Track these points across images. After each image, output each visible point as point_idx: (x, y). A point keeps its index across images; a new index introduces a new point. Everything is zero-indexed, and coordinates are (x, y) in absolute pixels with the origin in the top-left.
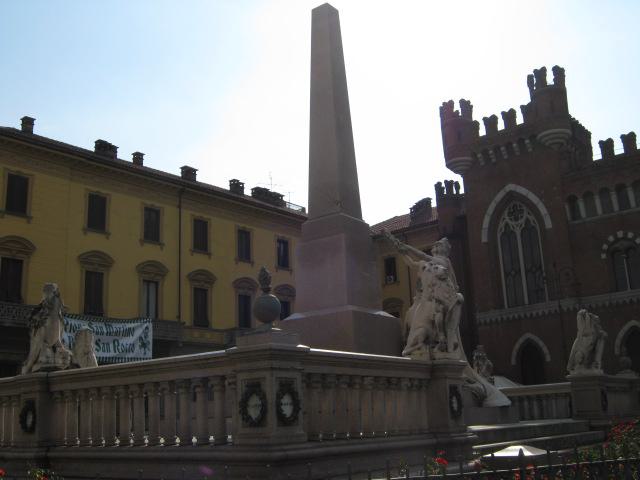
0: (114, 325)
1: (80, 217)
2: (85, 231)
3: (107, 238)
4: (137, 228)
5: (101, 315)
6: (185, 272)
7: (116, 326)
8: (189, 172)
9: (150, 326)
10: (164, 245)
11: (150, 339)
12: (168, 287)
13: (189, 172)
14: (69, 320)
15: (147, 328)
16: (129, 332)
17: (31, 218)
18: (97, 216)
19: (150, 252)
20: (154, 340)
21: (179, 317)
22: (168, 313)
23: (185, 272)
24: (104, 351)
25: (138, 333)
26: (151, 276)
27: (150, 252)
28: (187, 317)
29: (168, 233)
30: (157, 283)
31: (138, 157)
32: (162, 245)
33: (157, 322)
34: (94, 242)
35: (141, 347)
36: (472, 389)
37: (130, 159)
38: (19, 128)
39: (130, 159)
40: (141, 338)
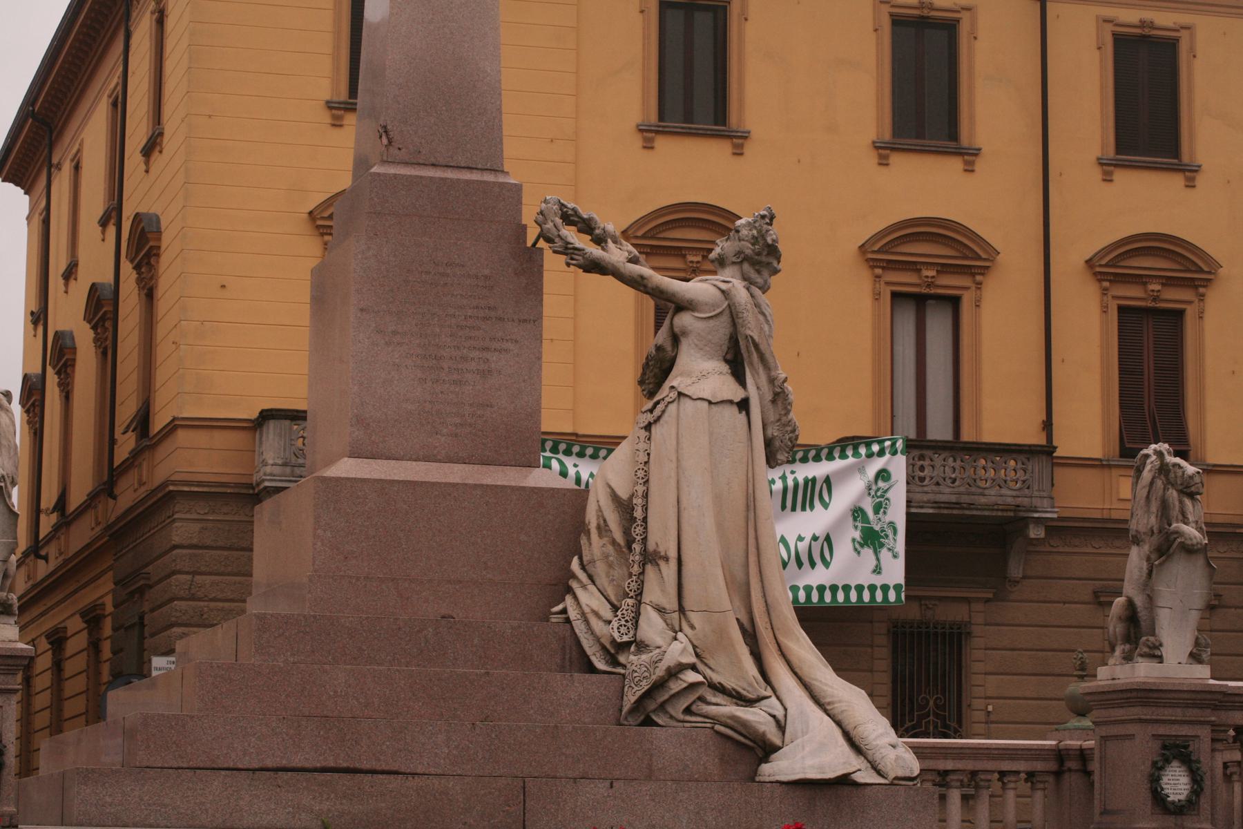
1: (630, 91)
2: (648, 134)
3: (738, 152)
4: (860, 91)
6: (1072, 255)
9: (898, 466)
11: (897, 514)
12: (1001, 316)
14: (569, 462)
15: (883, 474)
16: (807, 495)
19: (924, 188)
20: (911, 518)
21: (1048, 425)
22: (1003, 416)
23: (1072, 255)
25: (848, 494)
26: (926, 276)
27: (924, 188)
28: (1086, 426)
29: (993, 101)
30: (954, 302)
33: (918, 447)
34: (690, 171)
35: (859, 546)
36: (715, 719)
40: (857, 513)
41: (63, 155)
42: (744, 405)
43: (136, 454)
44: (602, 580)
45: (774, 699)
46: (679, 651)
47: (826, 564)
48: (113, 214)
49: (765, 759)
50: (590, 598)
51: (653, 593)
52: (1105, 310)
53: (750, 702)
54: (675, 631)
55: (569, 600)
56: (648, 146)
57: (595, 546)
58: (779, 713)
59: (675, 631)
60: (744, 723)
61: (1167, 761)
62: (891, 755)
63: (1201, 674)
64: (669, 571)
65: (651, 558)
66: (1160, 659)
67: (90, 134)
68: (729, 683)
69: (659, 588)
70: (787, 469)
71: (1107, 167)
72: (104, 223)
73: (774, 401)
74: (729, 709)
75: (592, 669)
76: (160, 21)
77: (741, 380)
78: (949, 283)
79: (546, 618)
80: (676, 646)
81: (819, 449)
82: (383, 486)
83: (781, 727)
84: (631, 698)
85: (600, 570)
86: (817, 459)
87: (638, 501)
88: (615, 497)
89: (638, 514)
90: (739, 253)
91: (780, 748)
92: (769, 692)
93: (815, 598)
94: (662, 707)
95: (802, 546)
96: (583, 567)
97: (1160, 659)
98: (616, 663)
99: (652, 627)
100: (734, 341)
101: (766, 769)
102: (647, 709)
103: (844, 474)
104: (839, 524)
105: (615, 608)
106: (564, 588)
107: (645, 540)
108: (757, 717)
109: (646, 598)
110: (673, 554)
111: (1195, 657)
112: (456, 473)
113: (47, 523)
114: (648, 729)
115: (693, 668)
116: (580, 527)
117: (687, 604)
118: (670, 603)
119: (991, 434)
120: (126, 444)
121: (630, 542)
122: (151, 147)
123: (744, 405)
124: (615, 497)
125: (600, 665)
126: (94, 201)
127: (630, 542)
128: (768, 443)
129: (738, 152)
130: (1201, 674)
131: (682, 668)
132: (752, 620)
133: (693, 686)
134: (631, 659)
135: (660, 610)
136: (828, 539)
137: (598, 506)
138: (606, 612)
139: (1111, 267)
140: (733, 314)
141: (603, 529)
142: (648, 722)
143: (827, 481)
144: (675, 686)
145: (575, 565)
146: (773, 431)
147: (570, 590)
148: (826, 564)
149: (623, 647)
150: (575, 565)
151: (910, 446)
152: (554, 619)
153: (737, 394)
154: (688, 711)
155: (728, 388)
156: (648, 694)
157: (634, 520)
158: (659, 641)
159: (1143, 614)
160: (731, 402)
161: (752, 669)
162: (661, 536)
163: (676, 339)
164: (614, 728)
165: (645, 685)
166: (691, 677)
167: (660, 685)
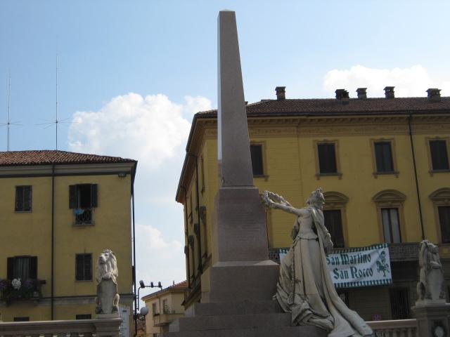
0: (349, 254)
1: (312, 165)
3: (340, 179)
4: (369, 162)
5: (343, 246)
6: (425, 195)
7: (351, 255)
8: (434, 93)
9: (387, 250)
10: (398, 173)
11: (388, 261)
12: (409, 211)
13: (434, 93)
15: (383, 253)
16: (365, 259)
17: (268, 176)
18: (328, 161)
19: (387, 182)
20: (391, 263)
23: (425, 195)
24: (342, 278)
25: (375, 257)
26: (389, 204)
27: (387, 182)
29: (401, 159)
30: (397, 209)
31: (389, 91)
32: (397, 174)
33: (391, 247)
34: (329, 184)
35: (379, 270)
36: (316, 323)
37: (383, 95)
38: (275, 98)
39: (383, 95)
41: (188, 195)
42: (317, 240)
43: (205, 262)
44: (285, 288)
45: (331, 317)
46: (305, 305)
47: (371, 275)
48: (197, 208)
49: (330, 333)
50: (281, 293)
51: (297, 291)
52: (434, 208)
53: (325, 318)
54: (304, 300)
55: (277, 294)
56: (318, 179)
57: (282, 280)
58: (332, 320)
59: (304, 300)
60: (323, 323)
61: (436, 327)
62: (364, 329)
63: (444, 302)
64: (301, 284)
65: (296, 281)
66: (431, 299)
67: (193, 189)
68: (319, 313)
69: (299, 289)
70: (359, 252)
71: (431, 173)
72: (196, 209)
73: (325, 238)
74: (318, 320)
75: (284, 312)
76: (203, 162)
77: (316, 234)
78: (395, 205)
79: (272, 299)
80: (304, 304)
81: (357, 248)
82: (227, 269)
83: (333, 324)
84: (293, 318)
85: (284, 286)
86: (366, 250)
87: (292, 267)
88: (287, 267)
89: (293, 270)
90: (313, 200)
91: (332, 330)
92: (328, 314)
93: (366, 284)
94: (302, 320)
95: (365, 271)
96: (280, 285)
97: (431, 299)
98: (289, 309)
99: (298, 299)
100: (313, 223)
101: (329, 335)
102: (297, 322)
103: (374, 253)
104: (373, 266)
105: (288, 295)
106: (275, 291)
107: (295, 277)
108: (326, 321)
109: (296, 292)
110: (302, 280)
111: (441, 297)
112: (242, 264)
113: (191, 280)
114: (297, 327)
115: (309, 310)
116: (278, 275)
117: (307, 293)
118: (302, 293)
119: (410, 240)
120: (203, 259)
121: (291, 277)
122: (203, 191)
123: (317, 240)
124: (287, 267)
125: (285, 311)
126: (194, 206)
127: (291, 277)
128: (325, 249)
129: (340, 179)
130: (444, 302)
131: (306, 310)
132: (324, 296)
133: (309, 314)
134: (293, 308)
135: (299, 295)
136: (371, 269)
137: (282, 269)
138: (286, 297)
139: (435, 197)
140: (312, 216)
141: (284, 275)
142: (298, 325)
143: (369, 255)
144: (304, 315)
145: (278, 285)
146: (326, 246)
147: (277, 291)
148: (371, 275)
149: (291, 305)
150: (278, 285)
151: (388, 246)
152: (274, 299)
153: (315, 237)
154: (308, 321)
155: (312, 235)
156: (298, 317)
157: (291, 271)
158: (300, 303)
159: (426, 287)
160: (313, 239)
161: (324, 308)
162: (298, 276)
163: (299, 224)
164: (289, 327)
165: (296, 315)
166: (309, 312)
167: (300, 315)
